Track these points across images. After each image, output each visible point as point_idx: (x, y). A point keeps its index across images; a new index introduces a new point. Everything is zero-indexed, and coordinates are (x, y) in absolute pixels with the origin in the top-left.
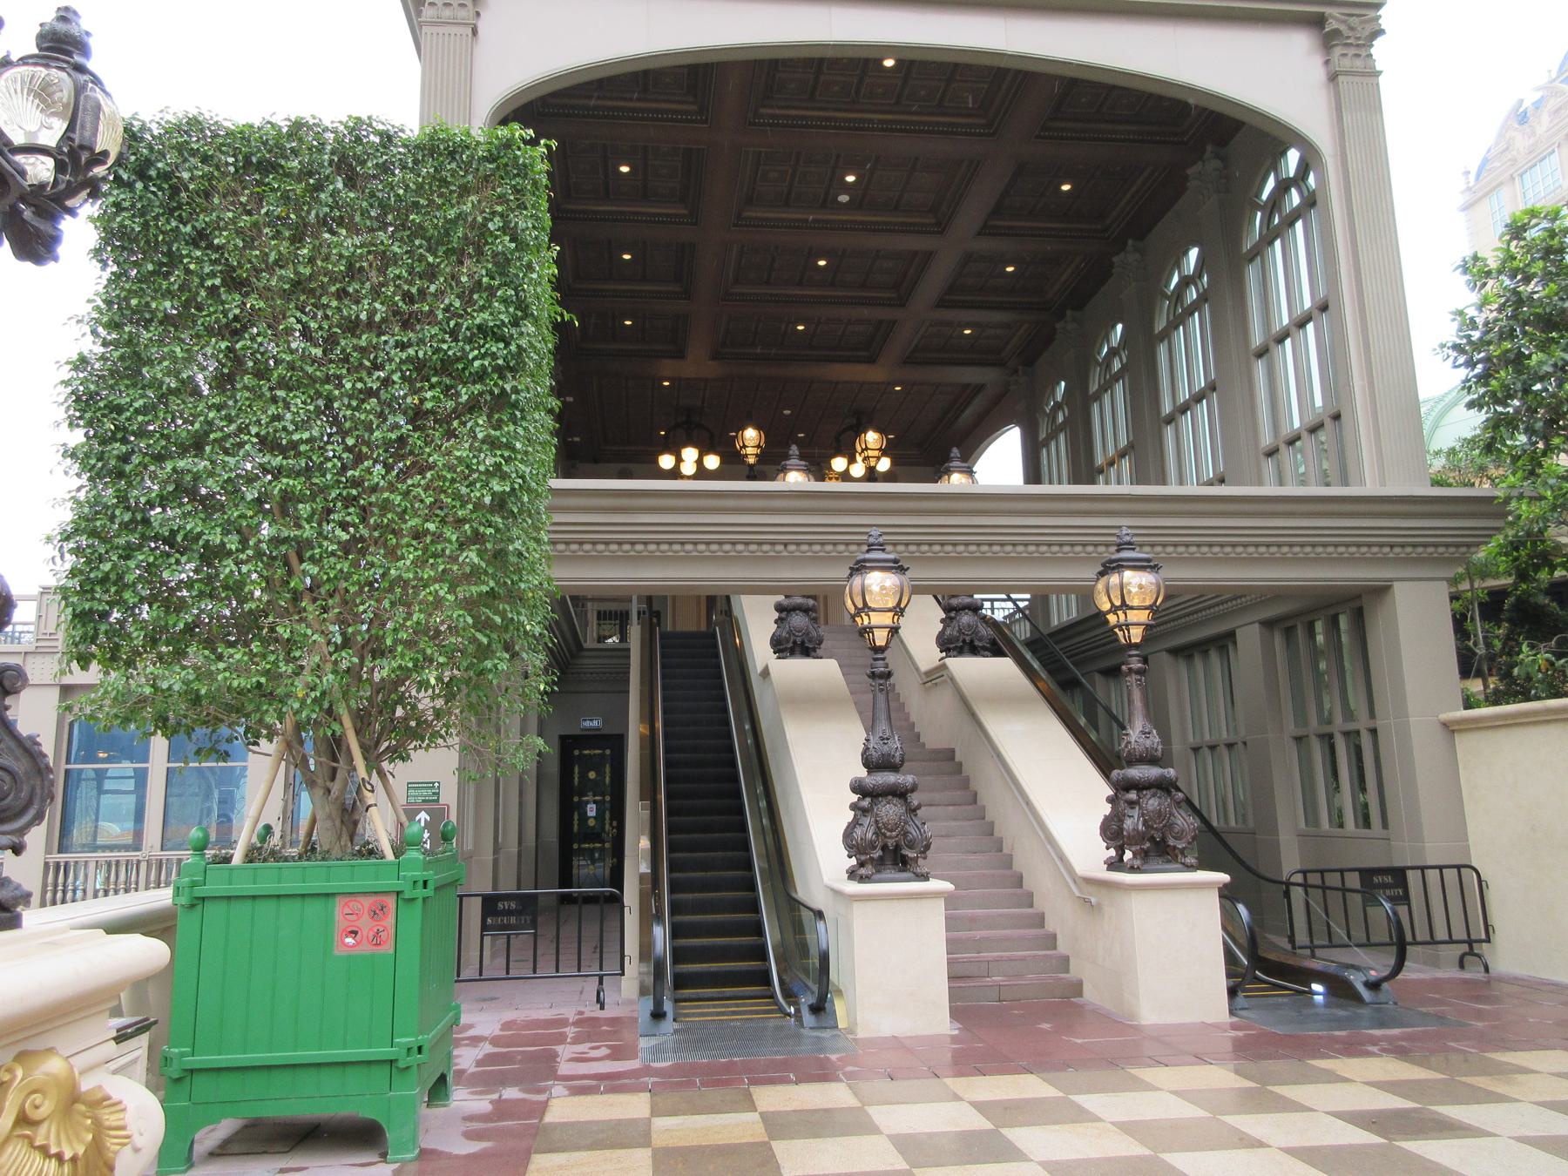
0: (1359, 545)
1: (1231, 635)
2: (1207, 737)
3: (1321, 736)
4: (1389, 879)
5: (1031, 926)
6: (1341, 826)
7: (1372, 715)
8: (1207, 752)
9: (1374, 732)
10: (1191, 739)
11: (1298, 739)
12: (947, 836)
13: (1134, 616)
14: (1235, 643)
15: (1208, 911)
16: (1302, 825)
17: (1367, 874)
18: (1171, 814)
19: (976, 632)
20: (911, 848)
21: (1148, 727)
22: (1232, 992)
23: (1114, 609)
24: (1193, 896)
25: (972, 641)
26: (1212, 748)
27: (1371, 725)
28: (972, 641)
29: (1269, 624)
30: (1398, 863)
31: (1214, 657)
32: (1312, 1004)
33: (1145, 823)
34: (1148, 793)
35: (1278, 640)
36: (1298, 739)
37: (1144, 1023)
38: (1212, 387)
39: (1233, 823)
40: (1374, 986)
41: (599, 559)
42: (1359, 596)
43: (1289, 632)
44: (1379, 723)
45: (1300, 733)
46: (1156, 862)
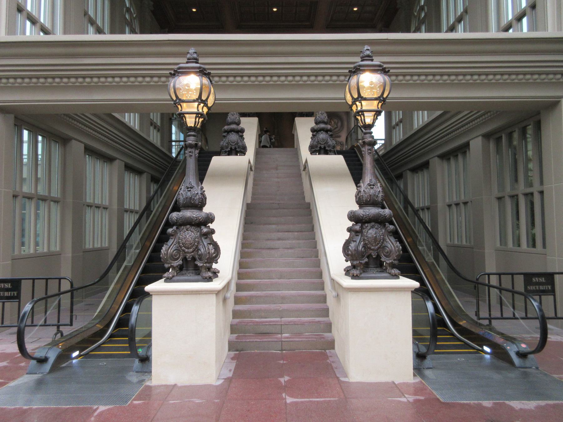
0: (540, 74)
1: (467, 145)
2: (455, 199)
3: (512, 197)
4: (543, 280)
5: (319, 302)
6: (519, 246)
7: (542, 183)
8: (454, 207)
9: (542, 193)
10: (447, 201)
11: (499, 199)
12: (291, 248)
13: (366, 105)
14: (469, 149)
15: (405, 305)
16: (498, 244)
17: (528, 277)
18: (384, 240)
19: (327, 143)
20: (200, 259)
21: (374, 181)
22: (420, 357)
23: (355, 101)
24: (392, 297)
25: (325, 148)
26: (457, 204)
27: (540, 189)
28: (325, 148)
29: (487, 136)
30: (550, 270)
31: (460, 158)
32: (482, 358)
33: (365, 246)
34: (369, 225)
35: (492, 145)
36: (499, 199)
37: (352, 380)
38: (466, 11)
39: (464, 243)
40: (522, 355)
41: (66, 88)
42: (539, 113)
43: (498, 140)
44: (545, 188)
45: (500, 195)
46: (373, 272)
